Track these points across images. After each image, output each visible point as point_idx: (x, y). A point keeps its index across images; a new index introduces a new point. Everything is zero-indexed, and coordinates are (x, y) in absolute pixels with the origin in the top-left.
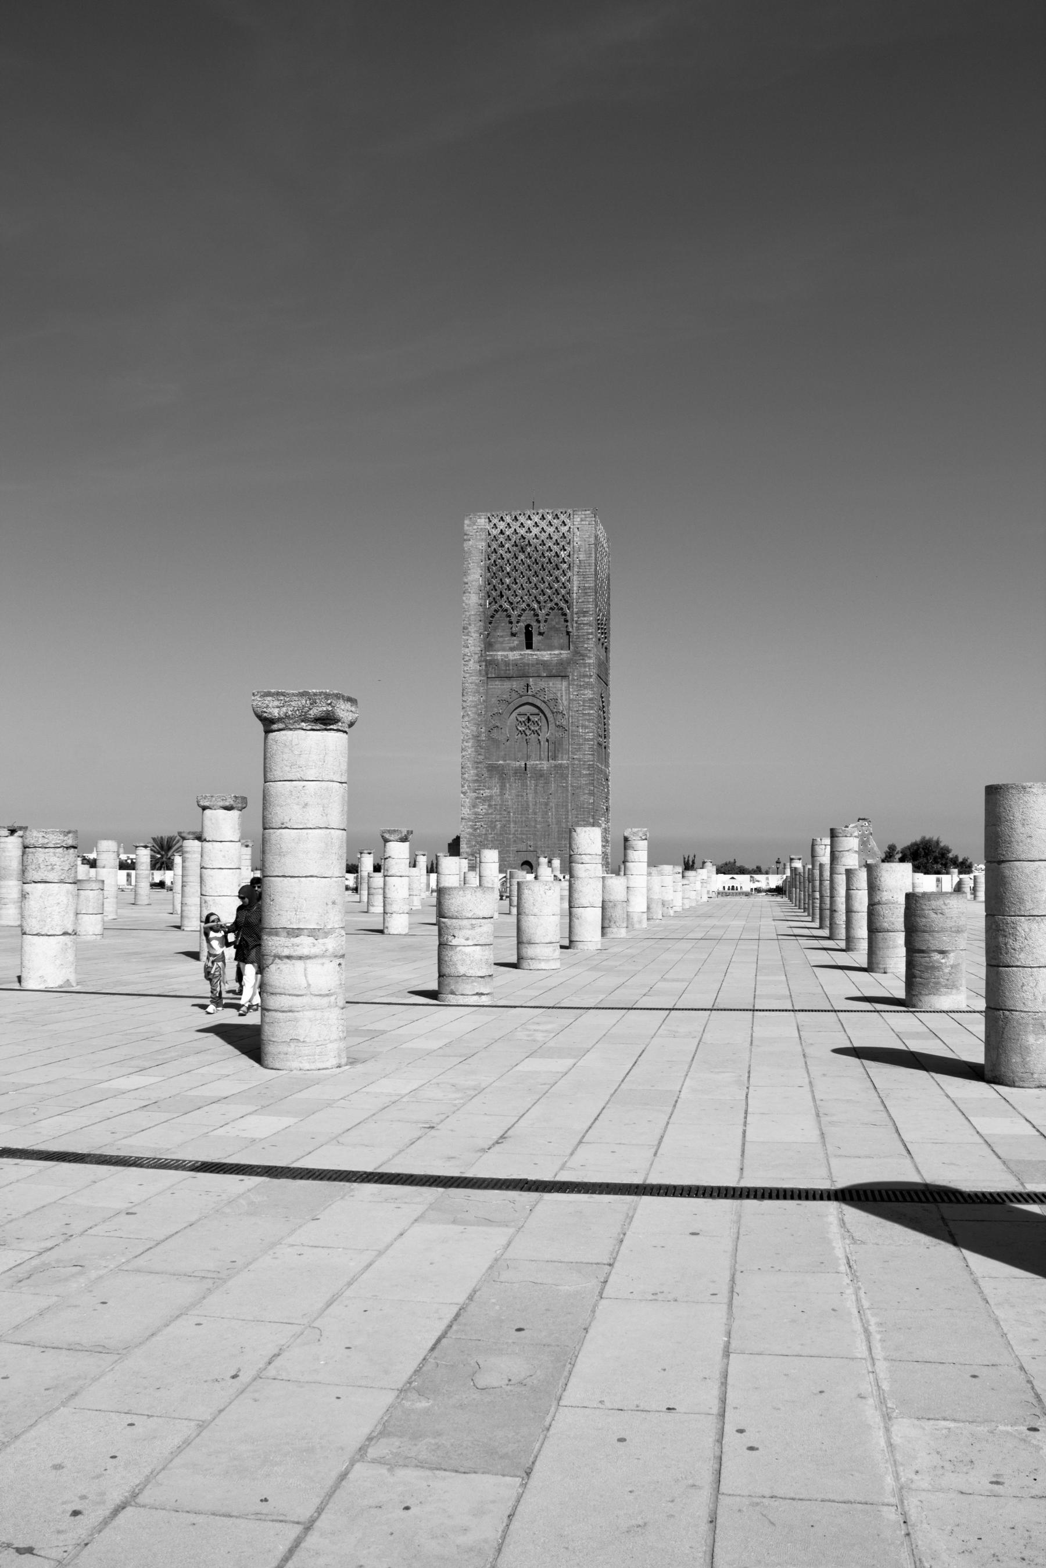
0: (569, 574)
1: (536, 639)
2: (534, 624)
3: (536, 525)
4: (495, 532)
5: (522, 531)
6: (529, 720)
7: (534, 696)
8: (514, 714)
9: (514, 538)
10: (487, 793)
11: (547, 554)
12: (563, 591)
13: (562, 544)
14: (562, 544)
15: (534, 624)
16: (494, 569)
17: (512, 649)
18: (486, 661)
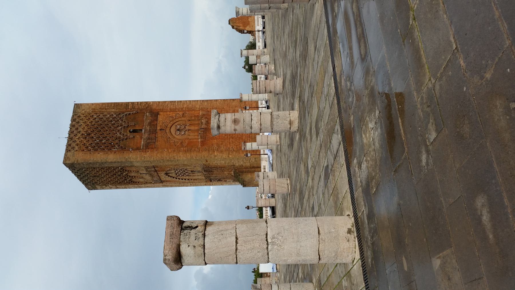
0: (105, 113)
1: (137, 128)
2: (129, 129)
3: (77, 129)
4: (77, 148)
5: (79, 135)
6: (178, 130)
7: (167, 127)
8: (176, 136)
9: (82, 139)
10: (215, 146)
11: (93, 123)
12: (115, 116)
13: (89, 117)
14: (89, 117)
15: (129, 129)
16: (97, 148)
17: (141, 138)
18: (146, 149)
